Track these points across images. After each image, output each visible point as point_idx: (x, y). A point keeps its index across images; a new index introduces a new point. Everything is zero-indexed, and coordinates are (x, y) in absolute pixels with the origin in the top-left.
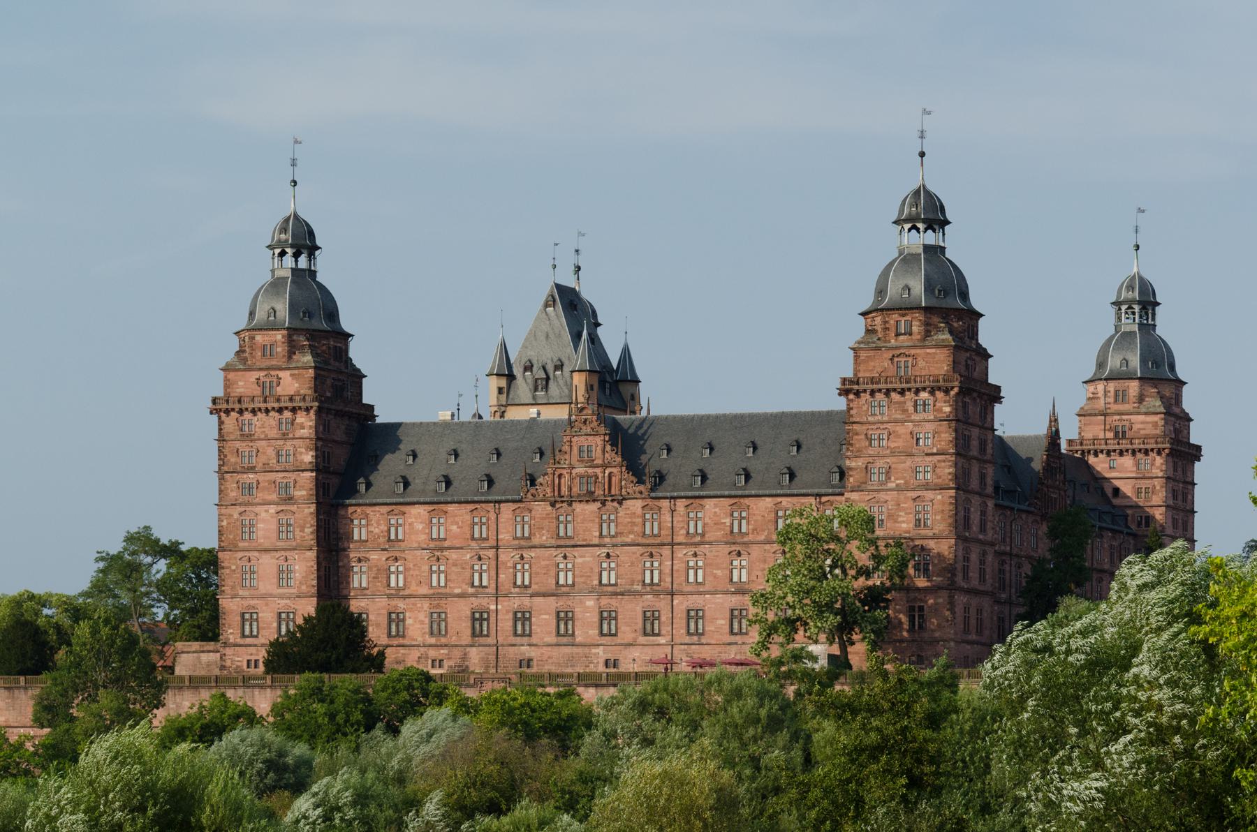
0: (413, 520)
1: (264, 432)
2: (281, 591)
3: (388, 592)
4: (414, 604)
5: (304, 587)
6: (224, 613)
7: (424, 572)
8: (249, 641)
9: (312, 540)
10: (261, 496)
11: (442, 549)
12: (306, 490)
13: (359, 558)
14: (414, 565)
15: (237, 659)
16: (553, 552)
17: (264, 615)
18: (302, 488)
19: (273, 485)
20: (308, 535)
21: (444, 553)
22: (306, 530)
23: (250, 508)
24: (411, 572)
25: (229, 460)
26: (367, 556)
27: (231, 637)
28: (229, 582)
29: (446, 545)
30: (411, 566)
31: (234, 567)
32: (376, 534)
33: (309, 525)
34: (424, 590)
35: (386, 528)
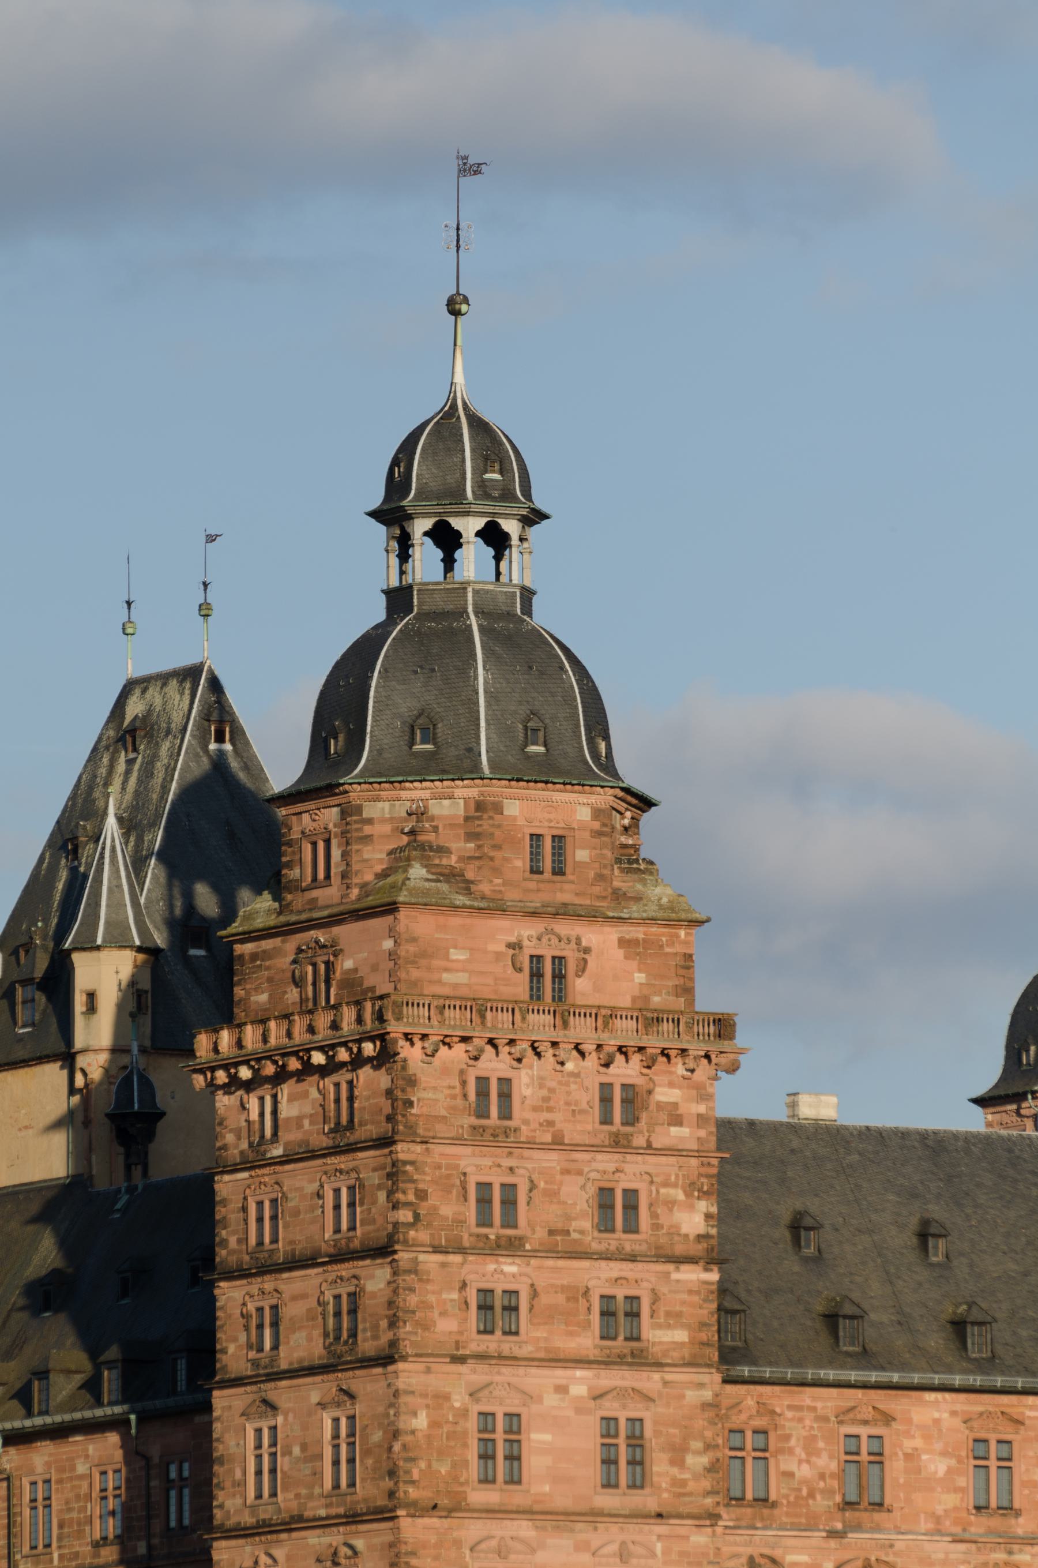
0: (918, 1442)
1: (550, 1123)
9: (708, 1493)
18: (674, 1318)
19: (582, 1302)
20: (696, 1477)
22: (690, 1460)
23: (507, 1374)
25: (435, 1208)
26: (777, 1553)
29: (1020, 1532)
32: (805, 1481)
33: (697, 1445)
35: (834, 1466)
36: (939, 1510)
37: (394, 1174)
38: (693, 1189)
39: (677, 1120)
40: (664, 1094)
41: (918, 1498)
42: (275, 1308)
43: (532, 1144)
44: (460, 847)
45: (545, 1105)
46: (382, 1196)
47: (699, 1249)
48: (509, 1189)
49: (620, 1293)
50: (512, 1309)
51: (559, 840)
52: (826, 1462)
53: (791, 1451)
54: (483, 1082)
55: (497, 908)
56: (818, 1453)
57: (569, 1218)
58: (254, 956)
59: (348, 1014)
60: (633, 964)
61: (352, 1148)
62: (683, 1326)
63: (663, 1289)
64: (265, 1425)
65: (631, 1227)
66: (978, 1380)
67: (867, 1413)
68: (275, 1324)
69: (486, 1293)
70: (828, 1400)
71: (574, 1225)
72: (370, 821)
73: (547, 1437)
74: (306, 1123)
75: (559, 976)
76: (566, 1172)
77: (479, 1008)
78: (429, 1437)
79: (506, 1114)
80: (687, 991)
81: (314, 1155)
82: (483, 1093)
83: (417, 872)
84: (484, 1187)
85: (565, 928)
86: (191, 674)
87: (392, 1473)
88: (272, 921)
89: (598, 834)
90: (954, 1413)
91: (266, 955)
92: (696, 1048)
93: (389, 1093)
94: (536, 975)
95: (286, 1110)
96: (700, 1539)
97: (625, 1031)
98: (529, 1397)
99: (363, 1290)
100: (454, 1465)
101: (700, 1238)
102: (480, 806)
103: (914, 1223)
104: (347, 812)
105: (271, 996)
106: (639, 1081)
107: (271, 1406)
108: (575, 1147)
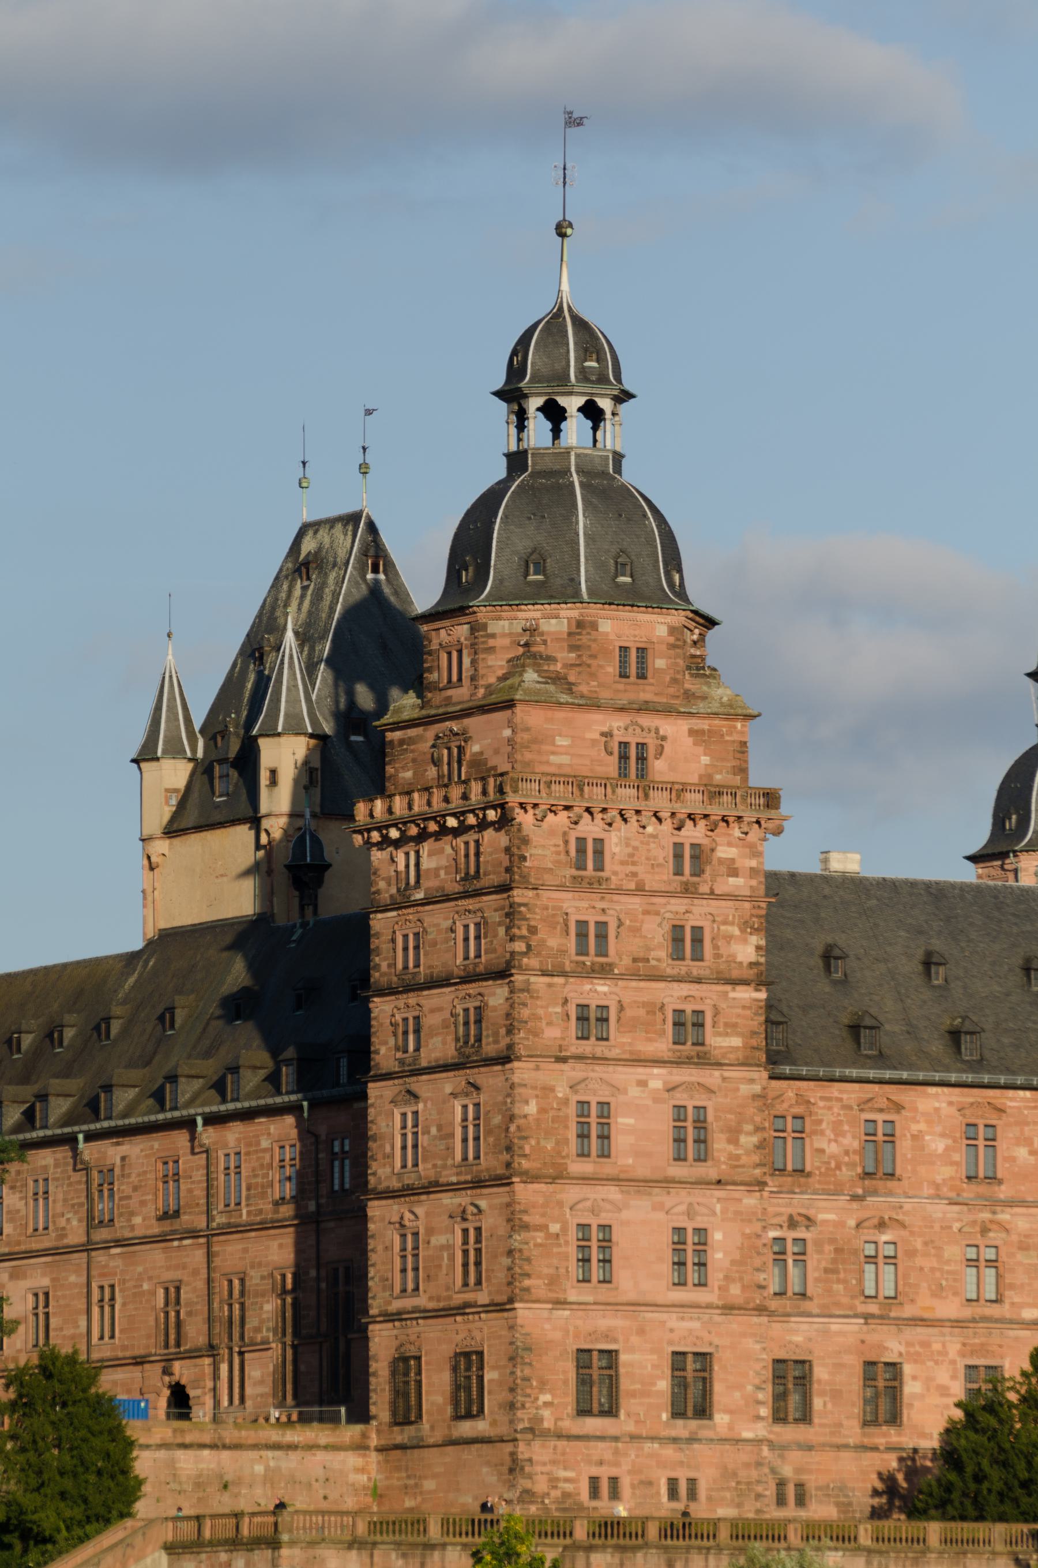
0: (922, 1126)
1: (635, 874)
3: (861, 1308)
4: (925, 1344)
5: (735, 1290)
6: (529, 1349)
7: (948, 1262)
8: (593, 1424)
9: (758, 1165)
10: (620, 1041)
11: (994, 1204)
12: (741, 1034)
13: (791, 1218)
14: (926, 1244)
15: (562, 1474)
17: (637, 1357)
18: (731, 1028)
19: (659, 1015)
20: (748, 1153)
21: (1004, 1216)
22: (743, 1139)
23: (599, 1071)
24: (919, 1261)
25: (544, 941)
26: (811, 1213)
27: (546, 1413)
28: (543, 1267)
29: (1002, 1196)
30: (918, 1244)
31: (555, 1228)
32: (833, 1156)
33: (748, 1127)
34: (949, 1308)
35: (856, 1144)
36: (939, 1179)
37: (511, 914)
38: (746, 926)
39: (734, 872)
40: (724, 852)
41: (922, 1170)
42: (417, 1018)
43: (620, 891)
44: (564, 656)
45: (630, 859)
46: (502, 931)
47: (751, 973)
48: (602, 926)
49: (689, 1008)
50: (604, 1020)
51: (642, 651)
52: (851, 1142)
53: (822, 1133)
54: (581, 841)
55: (593, 704)
56: (843, 1134)
57: (649, 949)
58: (402, 742)
59: (476, 788)
60: (700, 749)
61: (478, 893)
62: (738, 1034)
63: (723, 1005)
64: (409, 1110)
65: (698, 957)
66: (969, 1077)
67: (883, 1103)
68: (417, 1032)
69: (583, 1007)
70: (851, 1093)
71: (653, 954)
72: (493, 636)
73: (631, 1121)
74: (442, 873)
75: (642, 759)
76: (646, 912)
77: (579, 783)
78: (538, 1120)
79: (599, 867)
80: (742, 770)
81: (447, 898)
82: (581, 850)
83: (531, 676)
84: (582, 925)
85: (647, 720)
86: (353, 519)
87: (509, 1149)
88: (416, 714)
89: (672, 646)
90: (950, 1103)
91: (411, 741)
92: (750, 816)
93: (507, 850)
94: (624, 757)
95: (426, 863)
96: (751, 1201)
97: (694, 802)
98: (616, 1089)
99: (486, 1004)
100: (558, 1143)
101: (751, 965)
102: (580, 624)
103: (920, 954)
104: (476, 628)
105: (415, 774)
106: (705, 841)
107: (413, 1096)
108: (654, 893)
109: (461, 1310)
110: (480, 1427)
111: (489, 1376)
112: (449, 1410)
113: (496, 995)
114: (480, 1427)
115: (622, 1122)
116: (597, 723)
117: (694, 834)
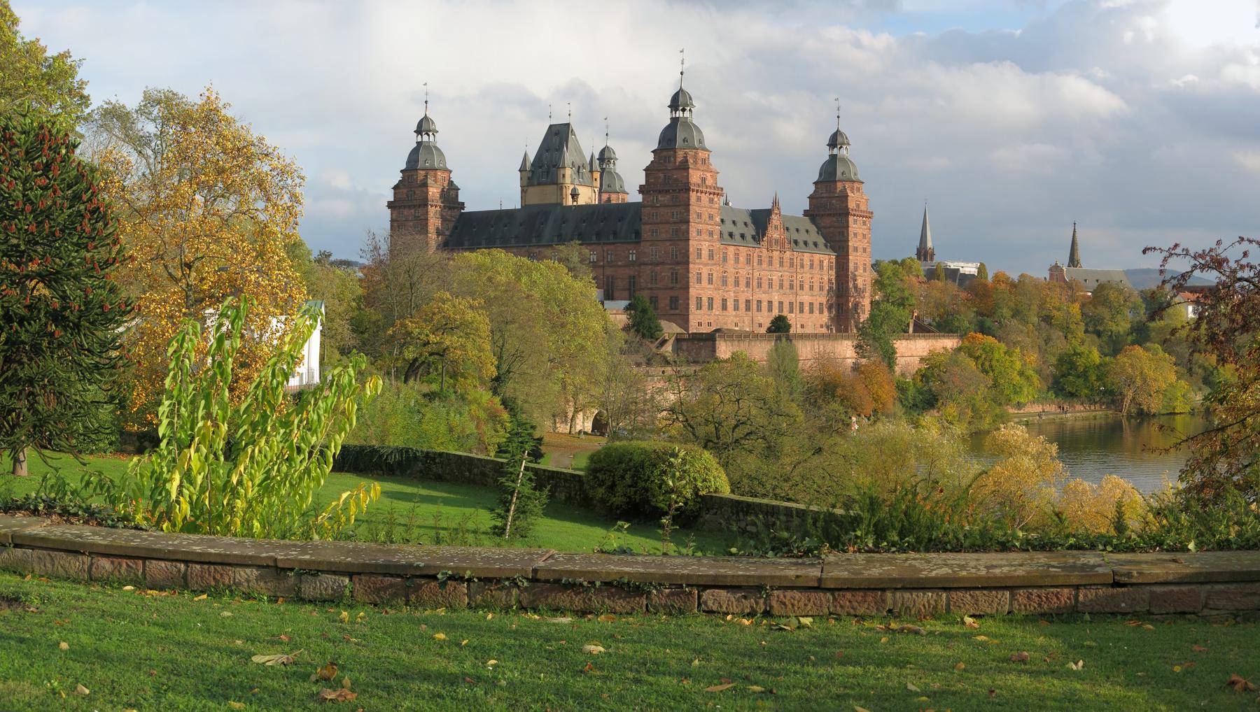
2: (710, 286)
16: (769, 273)
40: (716, 199)
55: (699, 170)
80: (716, 184)
109: (672, 288)
110: (677, 312)
111: (681, 302)
112: (668, 308)
113: (684, 227)
114: (677, 312)
115: (703, 252)
116: (700, 173)
117: (712, 196)
